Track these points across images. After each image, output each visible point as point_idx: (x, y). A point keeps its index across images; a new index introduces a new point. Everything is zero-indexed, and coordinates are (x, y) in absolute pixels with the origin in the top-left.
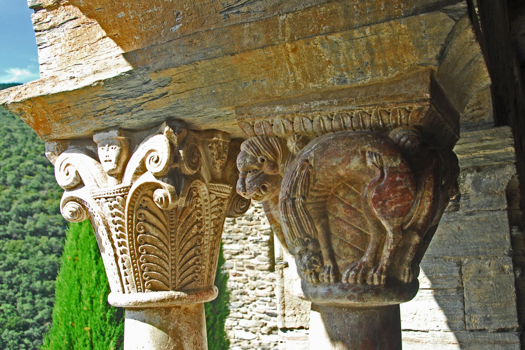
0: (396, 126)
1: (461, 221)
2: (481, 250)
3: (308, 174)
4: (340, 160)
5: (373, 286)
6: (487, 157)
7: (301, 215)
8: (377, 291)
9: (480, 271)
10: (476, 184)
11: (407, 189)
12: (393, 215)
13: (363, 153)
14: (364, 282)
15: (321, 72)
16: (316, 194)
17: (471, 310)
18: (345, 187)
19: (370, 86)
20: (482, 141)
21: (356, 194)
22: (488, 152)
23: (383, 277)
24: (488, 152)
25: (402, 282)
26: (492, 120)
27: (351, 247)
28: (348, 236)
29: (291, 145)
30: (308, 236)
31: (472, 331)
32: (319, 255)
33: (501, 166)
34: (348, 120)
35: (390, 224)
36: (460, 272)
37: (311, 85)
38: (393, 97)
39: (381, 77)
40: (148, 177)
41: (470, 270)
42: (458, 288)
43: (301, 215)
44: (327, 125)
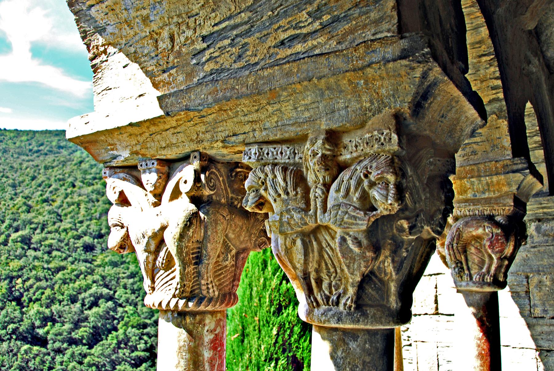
0: (498, 215)
1: (528, 251)
2: (541, 269)
3: (459, 234)
4: (474, 229)
5: (487, 283)
6: (545, 213)
7: (456, 251)
8: (489, 285)
9: (540, 282)
10: (538, 229)
11: (503, 242)
12: (497, 252)
13: (484, 226)
14: (483, 280)
15: (465, 192)
16: (462, 243)
17: (534, 305)
18: (475, 240)
19: (487, 198)
20: (541, 204)
21: (480, 243)
22: (545, 210)
23: (492, 278)
24: (545, 210)
25: (500, 281)
26: (548, 191)
27: (477, 265)
28: (476, 261)
30: (458, 260)
31: (535, 318)
34: (477, 212)
35: (496, 256)
36: (528, 282)
37: (461, 197)
38: (497, 204)
39: (492, 195)
41: (534, 280)
42: (526, 292)
43: (456, 251)
44: (468, 213)
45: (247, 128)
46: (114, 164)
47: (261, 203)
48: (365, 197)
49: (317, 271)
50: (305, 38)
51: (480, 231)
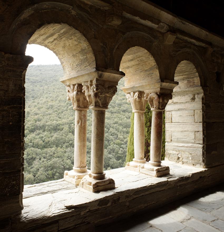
6: (199, 92)
12: (157, 101)
22: (199, 91)
24: (199, 91)
29: (149, 94)
32: (152, 105)
33: (201, 93)
40: (136, 97)
45: (82, 80)
46: (67, 85)
47: (84, 91)
48: (93, 90)
49: (91, 101)
50: (88, 66)
51: (154, 96)
